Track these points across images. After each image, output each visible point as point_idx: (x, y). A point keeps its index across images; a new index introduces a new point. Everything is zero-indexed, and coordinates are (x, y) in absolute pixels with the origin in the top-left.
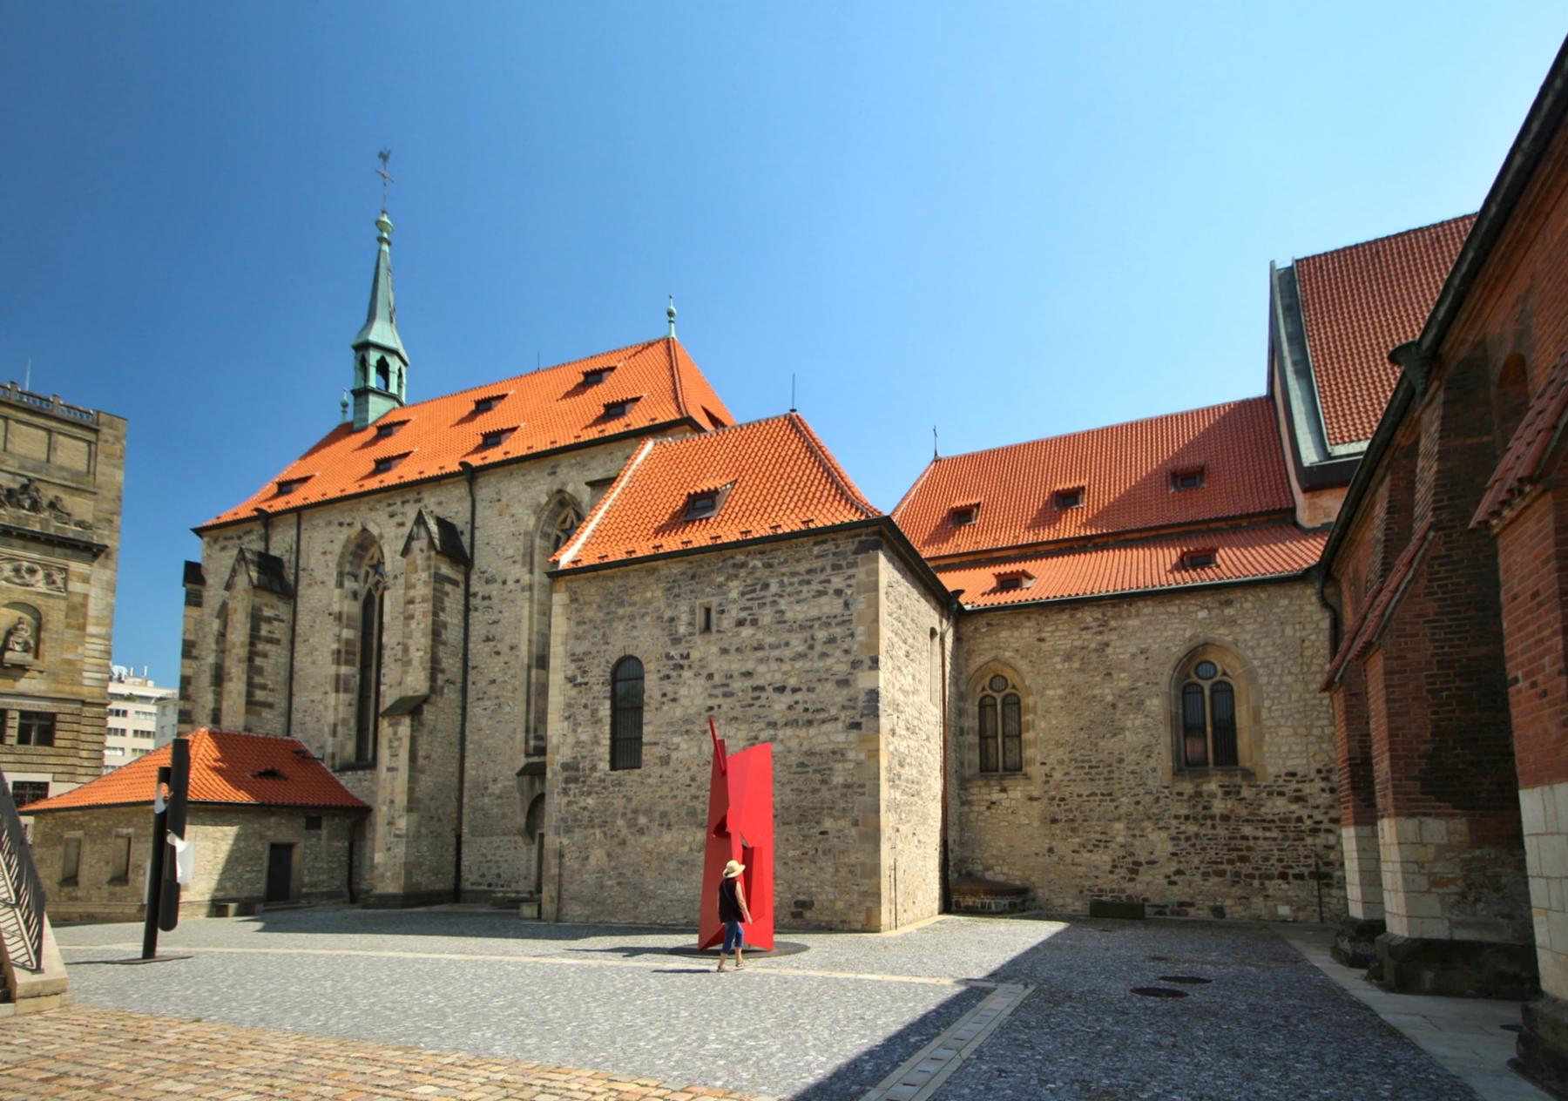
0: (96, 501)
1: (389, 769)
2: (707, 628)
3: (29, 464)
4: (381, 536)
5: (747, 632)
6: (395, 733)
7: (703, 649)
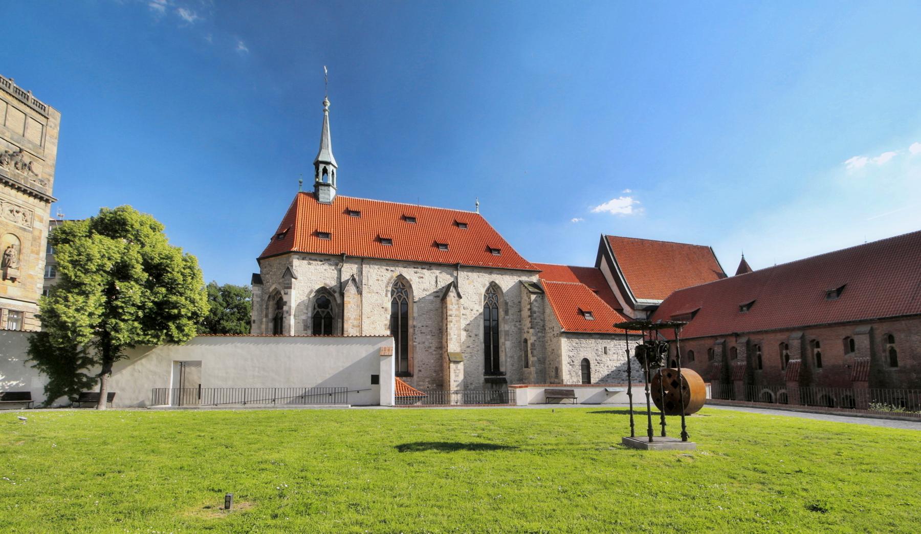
0: (43, 166)
1: (455, 381)
2: (605, 353)
3: (16, 137)
4: (411, 280)
5: (616, 356)
6: (457, 367)
7: (605, 358)
